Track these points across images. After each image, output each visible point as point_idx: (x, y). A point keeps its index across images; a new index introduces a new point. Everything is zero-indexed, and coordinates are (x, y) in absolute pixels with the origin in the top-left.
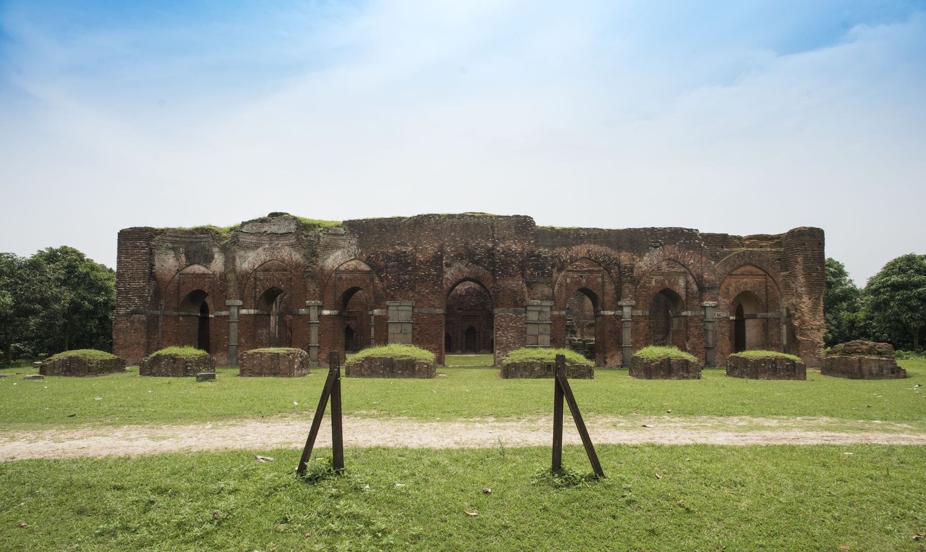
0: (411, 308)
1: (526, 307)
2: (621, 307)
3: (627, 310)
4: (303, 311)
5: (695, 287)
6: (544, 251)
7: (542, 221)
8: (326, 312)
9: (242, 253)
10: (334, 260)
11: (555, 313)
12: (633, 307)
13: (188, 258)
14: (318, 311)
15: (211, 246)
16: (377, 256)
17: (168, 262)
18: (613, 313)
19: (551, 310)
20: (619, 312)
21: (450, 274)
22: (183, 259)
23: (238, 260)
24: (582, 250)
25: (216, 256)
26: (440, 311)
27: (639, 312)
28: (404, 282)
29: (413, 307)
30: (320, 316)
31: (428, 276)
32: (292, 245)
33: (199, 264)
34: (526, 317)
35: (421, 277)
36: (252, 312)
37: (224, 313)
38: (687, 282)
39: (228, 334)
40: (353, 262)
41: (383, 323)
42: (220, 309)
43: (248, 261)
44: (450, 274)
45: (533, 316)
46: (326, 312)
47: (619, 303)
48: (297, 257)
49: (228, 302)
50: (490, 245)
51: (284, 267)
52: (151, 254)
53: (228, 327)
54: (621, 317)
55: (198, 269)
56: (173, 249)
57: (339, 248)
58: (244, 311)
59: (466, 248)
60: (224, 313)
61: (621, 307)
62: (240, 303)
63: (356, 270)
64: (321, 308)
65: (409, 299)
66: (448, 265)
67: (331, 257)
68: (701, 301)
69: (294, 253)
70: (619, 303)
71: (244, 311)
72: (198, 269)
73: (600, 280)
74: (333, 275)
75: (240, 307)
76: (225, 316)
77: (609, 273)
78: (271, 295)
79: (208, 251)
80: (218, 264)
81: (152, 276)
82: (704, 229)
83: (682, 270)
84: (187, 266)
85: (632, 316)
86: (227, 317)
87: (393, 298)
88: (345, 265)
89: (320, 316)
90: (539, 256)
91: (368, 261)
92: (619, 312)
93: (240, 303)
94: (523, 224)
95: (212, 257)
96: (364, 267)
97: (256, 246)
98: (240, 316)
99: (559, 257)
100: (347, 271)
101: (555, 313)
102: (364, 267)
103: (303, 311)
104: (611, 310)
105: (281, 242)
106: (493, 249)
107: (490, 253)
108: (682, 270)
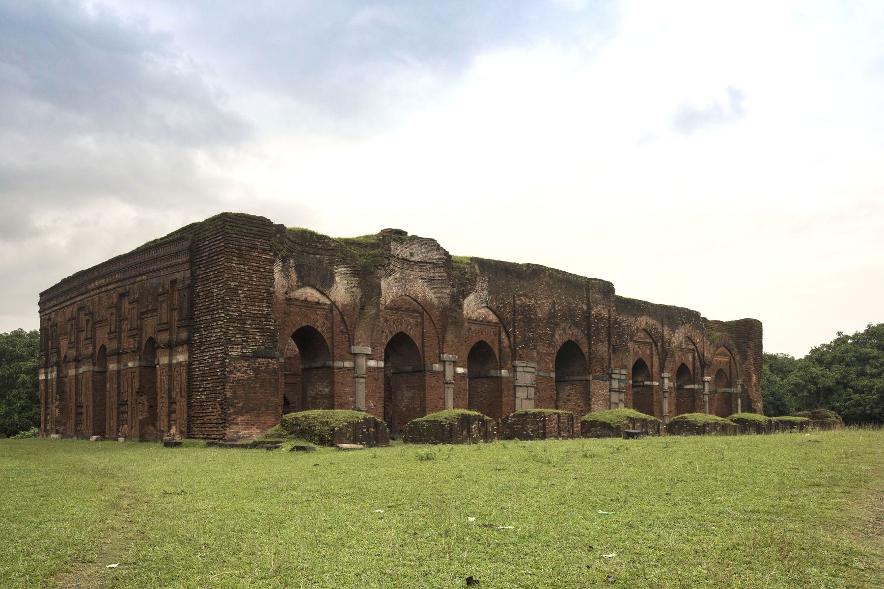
1: (610, 375)
4: (437, 367)
5: (698, 364)
7: (622, 291)
13: (301, 277)
15: (332, 263)
16: (505, 307)
22: (294, 276)
24: (643, 321)
25: (337, 279)
28: (529, 339)
31: (545, 334)
32: (431, 281)
33: (313, 287)
34: (610, 385)
35: (540, 335)
37: (347, 364)
38: (694, 358)
39: (354, 394)
40: (483, 311)
42: (343, 359)
46: (460, 370)
49: (356, 349)
51: (419, 308)
53: (354, 385)
55: (310, 294)
59: (569, 307)
60: (347, 364)
64: (455, 364)
65: (532, 359)
68: (703, 376)
69: (427, 290)
72: (310, 294)
76: (348, 369)
80: (342, 290)
83: (693, 347)
84: (299, 287)
87: (521, 358)
93: (369, 350)
96: (493, 318)
98: (370, 369)
103: (437, 367)
105: (413, 274)
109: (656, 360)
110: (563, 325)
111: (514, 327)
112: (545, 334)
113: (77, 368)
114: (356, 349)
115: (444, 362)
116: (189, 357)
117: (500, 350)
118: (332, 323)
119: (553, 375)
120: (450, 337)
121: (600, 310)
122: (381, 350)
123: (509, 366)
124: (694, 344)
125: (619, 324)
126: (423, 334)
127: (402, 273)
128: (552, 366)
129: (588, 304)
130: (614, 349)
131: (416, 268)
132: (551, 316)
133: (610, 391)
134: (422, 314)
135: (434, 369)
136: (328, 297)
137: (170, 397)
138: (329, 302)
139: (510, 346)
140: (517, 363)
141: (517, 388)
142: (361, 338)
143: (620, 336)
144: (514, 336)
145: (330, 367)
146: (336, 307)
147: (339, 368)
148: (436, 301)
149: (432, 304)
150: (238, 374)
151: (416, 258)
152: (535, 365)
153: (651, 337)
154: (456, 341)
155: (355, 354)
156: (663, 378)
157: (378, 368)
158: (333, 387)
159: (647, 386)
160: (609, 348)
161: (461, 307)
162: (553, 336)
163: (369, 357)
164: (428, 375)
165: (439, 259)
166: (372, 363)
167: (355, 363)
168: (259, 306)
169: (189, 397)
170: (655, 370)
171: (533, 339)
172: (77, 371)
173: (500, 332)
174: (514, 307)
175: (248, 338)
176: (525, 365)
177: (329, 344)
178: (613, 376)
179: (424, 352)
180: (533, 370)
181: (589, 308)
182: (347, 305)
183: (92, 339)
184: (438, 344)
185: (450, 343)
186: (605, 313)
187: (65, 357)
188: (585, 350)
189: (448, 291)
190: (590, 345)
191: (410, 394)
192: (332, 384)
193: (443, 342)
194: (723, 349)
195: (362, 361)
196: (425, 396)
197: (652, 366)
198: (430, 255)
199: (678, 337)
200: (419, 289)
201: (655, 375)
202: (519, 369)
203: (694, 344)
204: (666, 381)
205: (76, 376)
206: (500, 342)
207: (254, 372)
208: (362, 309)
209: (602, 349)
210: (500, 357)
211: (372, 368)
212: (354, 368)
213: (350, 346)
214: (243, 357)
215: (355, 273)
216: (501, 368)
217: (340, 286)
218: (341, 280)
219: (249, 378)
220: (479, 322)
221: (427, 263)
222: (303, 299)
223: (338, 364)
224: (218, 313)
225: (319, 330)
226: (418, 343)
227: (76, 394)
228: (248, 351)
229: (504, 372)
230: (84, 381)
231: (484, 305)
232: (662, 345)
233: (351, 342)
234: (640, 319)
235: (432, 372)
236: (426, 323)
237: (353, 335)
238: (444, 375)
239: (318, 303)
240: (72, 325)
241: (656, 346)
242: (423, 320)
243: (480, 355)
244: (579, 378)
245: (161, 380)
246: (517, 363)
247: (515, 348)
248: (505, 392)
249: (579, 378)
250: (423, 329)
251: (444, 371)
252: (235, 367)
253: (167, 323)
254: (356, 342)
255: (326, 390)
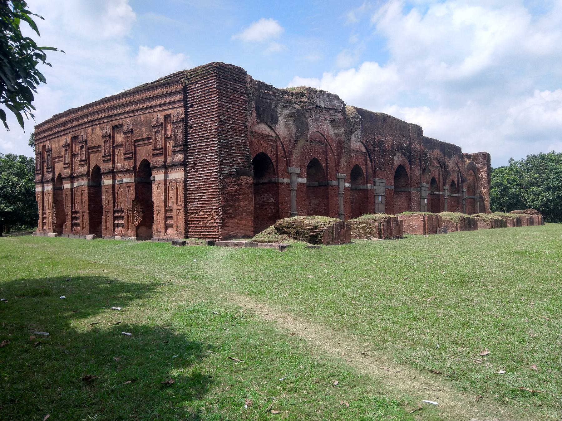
1: (420, 187)
4: (335, 182)
13: (259, 116)
16: (369, 141)
25: (280, 118)
30: (345, 188)
31: (390, 160)
32: (332, 121)
33: (266, 123)
38: (458, 177)
40: (358, 144)
42: (283, 177)
46: (347, 185)
49: (291, 169)
55: (263, 128)
60: (286, 180)
64: (345, 180)
69: (330, 128)
72: (263, 128)
79: (274, 110)
80: (284, 127)
83: (458, 170)
93: (298, 170)
96: (363, 149)
109: (441, 177)
110: (398, 154)
111: (374, 155)
112: (390, 160)
113: (72, 183)
114: (291, 169)
115: (339, 179)
116: (185, 175)
117: (367, 171)
118: (277, 151)
119: (393, 188)
120: (343, 162)
121: (416, 145)
122: (305, 170)
123: (372, 182)
124: (458, 167)
125: (425, 154)
126: (327, 159)
127: (316, 115)
128: (392, 181)
129: (410, 141)
130: (423, 171)
131: (323, 112)
132: (393, 148)
133: (421, 198)
134: (326, 146)
135: (333, 184)
136: (274, 131)
137: (166, 206)
138: (275, 135)
139: (372, 168)
140: (376, 180)
141: (376, 197)
142: (294, 161)
143: (426, 163)
144: (375, 161)
145: (275, 183)
146: (279, 139)
147: (282, 184)
148: (334, 136)
149: (332, 139)
150: (229, 188)
152: (384, 181)
153: (439, 162)
154: (345, 164)
155: (291, 173)
156: (445, 189)
157: (303, 184)
158: (277, 198)
159: (436, 194)
160: (420, 170)
161: (349, 140)
162: (393, 161)
163: (299, 176)
164: (330, 188)
165: (338, 106)
166: (300, 180)
167: (291, 180)
168: (240, 136)
169: (186, 206)
170: (441, 184)
171: (384, 163)
172: (72, 185)
173: (366, 158)
174: (375, 141)
175: (233, 161)
176: (380, 181)
177: (275, 167)
178: (422, 188)
179: (327, 173)
180: (384, 184)
181: (411, 143)
182: (285, 138)
183: (86, 161)
184: (335, 167)
185: (342, 166)
186: (418, 147)
187: (60, 174)
188: (408, 171)
189: (342, 129)
190: (411, 169)
191: (316, 202)
192: (277, 195)
193: (339, 165)
194: (471, 171)
195: (294, 178)
196: (328, 203)
197: (439, 182)
198: (332, 103)
199: (451, 164)
200: (325, 128)
201: (441, 188)
202: (377, 184)
203: (458, 167)
204: (446, 191)
205: (72, 189)
206: (366, 165)
207: (238, 186)
208: (296, 140)
209: (417, 171)
210: (367, 175)
211: (300, 183)
212: (290, 184)
213: (287, 167)
214: (231, 174)
215: (292, 114)
216: (367, 183)
217: (282, 123)
218: (282, 119)
219: (235, 191)
220: (356, 151)
221: (329, 109)
222: (260, 132)
223: (281, 180)
224: (213, 141)
225: (269, 155)
226: (324, 165)
227: (72, 203)
228: (234, 169)
229: (369, 186)
230: (80, 193)
231: (359, 140)
232: (445, 168)
233: (288, 164)
234: (435, 151)
235: (332, 186)
236: (329, 153)
237: (290, 160)
238: (339, 188)
239: (268, 136)
240: (66, 150)
241: (442, 169)
242: (327, 150)
243: (355, 174)
244: (403, 189)
245: (156, 191)
246: (376, 180)
247: (375, 170)
248: (370, 199)
249: (403, 189)
250: (327, 155)
251: (339, 185)
252: (227, 183)
253: (162, 149)
254: (291, 165)
255: (272, 199)
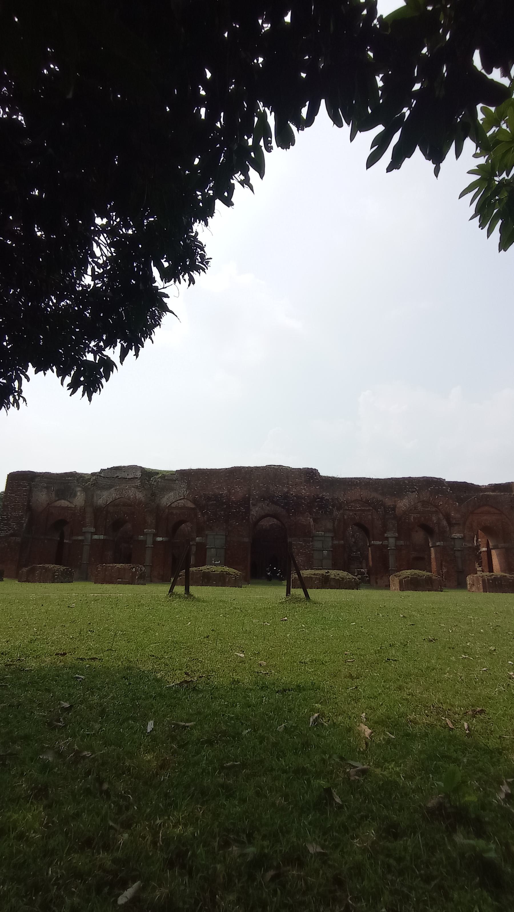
0: (224, 537)
1: (313, 537)
2: (387, 538)
3: (392, 541)
4: (141, 537)
6: (327, 495)
7: (324, 472)
8: (159, 539)
9: (99, 492)
10: (167, 499)
11: (336, 542)
12: (397, 539)
14: (151, 537)
17: (42, 497)
18: (381, 543)
19: (333, 540)
20: (385, 542)
21: (255, 511)
23: (95, 497)
25: (79, 494)
26: (246, 540)
27: (402, 543)
29: (226, 536)
30: (155, 542)
36: (102, 537)
37: (80, 538)
40: (182, 501)
41: (202, 548)
43: (104, 497)
44: (255, 511)
45: (318, 545)
46: (159, 539)
47: (386, 535)
48: (140, 496)
50: (286, 490)
52: (30, 491)
54: (387, 546)
55: (64, 503)
56: (47, 488)
57: (172, 489)
58: (96, 537)
60: (80, 538)
61: (387, 538)
62: (93, 530)
63: (184, 507)
64: (156, 535)
66: (254, 505)
67: (166, 497)
70: (386, 535)
71: (96, 537)
72: (64, 503)
73: (370, 517)
74: (167, 510)
75: (93, 534)
77: (377, 511)
78: (117, 525)
81: (29, 508)
82: (449, 477)
83: (434, 509)
85: (396, 546)
86: (82, 541)
88: (176, 503)
89: (155, 542)
90: (322, 498)
91: (194, 501)
92: (385, 542)
94: (311, 474)
95: (75, 495)
96: (190, 505)
97: (110, 487)
99: (337, 499)
100: (177, 508)
101: (336, 542)
102: (190, 505)
103: (141, 537)
104: (380, 541)
106: (287, 492)
107: (286, 496)
108: (434, 509)
135: (139, 539)
151: (130, 476)
195: (89, 536)
211: (96, 539)
239: (67, 507)
